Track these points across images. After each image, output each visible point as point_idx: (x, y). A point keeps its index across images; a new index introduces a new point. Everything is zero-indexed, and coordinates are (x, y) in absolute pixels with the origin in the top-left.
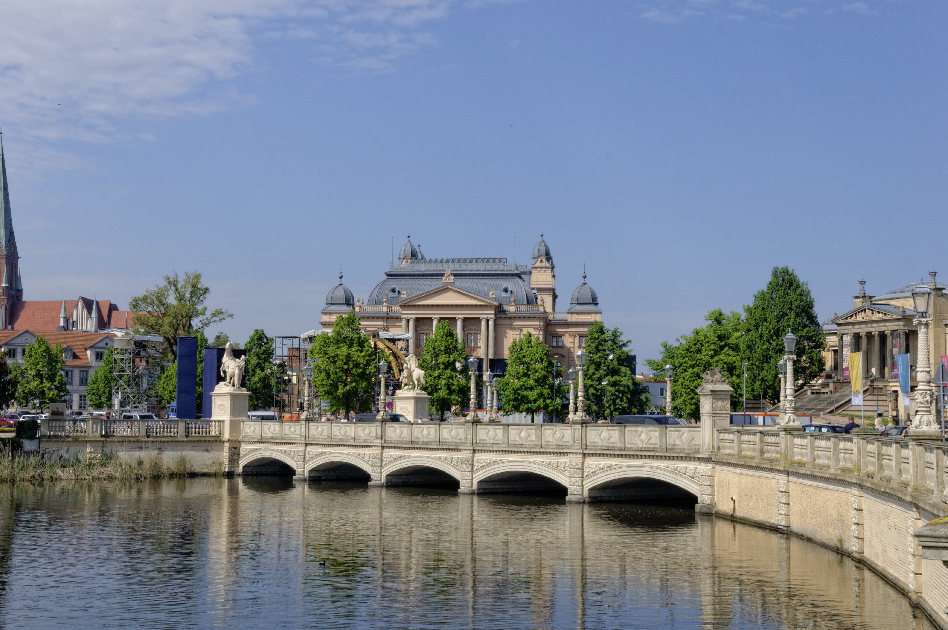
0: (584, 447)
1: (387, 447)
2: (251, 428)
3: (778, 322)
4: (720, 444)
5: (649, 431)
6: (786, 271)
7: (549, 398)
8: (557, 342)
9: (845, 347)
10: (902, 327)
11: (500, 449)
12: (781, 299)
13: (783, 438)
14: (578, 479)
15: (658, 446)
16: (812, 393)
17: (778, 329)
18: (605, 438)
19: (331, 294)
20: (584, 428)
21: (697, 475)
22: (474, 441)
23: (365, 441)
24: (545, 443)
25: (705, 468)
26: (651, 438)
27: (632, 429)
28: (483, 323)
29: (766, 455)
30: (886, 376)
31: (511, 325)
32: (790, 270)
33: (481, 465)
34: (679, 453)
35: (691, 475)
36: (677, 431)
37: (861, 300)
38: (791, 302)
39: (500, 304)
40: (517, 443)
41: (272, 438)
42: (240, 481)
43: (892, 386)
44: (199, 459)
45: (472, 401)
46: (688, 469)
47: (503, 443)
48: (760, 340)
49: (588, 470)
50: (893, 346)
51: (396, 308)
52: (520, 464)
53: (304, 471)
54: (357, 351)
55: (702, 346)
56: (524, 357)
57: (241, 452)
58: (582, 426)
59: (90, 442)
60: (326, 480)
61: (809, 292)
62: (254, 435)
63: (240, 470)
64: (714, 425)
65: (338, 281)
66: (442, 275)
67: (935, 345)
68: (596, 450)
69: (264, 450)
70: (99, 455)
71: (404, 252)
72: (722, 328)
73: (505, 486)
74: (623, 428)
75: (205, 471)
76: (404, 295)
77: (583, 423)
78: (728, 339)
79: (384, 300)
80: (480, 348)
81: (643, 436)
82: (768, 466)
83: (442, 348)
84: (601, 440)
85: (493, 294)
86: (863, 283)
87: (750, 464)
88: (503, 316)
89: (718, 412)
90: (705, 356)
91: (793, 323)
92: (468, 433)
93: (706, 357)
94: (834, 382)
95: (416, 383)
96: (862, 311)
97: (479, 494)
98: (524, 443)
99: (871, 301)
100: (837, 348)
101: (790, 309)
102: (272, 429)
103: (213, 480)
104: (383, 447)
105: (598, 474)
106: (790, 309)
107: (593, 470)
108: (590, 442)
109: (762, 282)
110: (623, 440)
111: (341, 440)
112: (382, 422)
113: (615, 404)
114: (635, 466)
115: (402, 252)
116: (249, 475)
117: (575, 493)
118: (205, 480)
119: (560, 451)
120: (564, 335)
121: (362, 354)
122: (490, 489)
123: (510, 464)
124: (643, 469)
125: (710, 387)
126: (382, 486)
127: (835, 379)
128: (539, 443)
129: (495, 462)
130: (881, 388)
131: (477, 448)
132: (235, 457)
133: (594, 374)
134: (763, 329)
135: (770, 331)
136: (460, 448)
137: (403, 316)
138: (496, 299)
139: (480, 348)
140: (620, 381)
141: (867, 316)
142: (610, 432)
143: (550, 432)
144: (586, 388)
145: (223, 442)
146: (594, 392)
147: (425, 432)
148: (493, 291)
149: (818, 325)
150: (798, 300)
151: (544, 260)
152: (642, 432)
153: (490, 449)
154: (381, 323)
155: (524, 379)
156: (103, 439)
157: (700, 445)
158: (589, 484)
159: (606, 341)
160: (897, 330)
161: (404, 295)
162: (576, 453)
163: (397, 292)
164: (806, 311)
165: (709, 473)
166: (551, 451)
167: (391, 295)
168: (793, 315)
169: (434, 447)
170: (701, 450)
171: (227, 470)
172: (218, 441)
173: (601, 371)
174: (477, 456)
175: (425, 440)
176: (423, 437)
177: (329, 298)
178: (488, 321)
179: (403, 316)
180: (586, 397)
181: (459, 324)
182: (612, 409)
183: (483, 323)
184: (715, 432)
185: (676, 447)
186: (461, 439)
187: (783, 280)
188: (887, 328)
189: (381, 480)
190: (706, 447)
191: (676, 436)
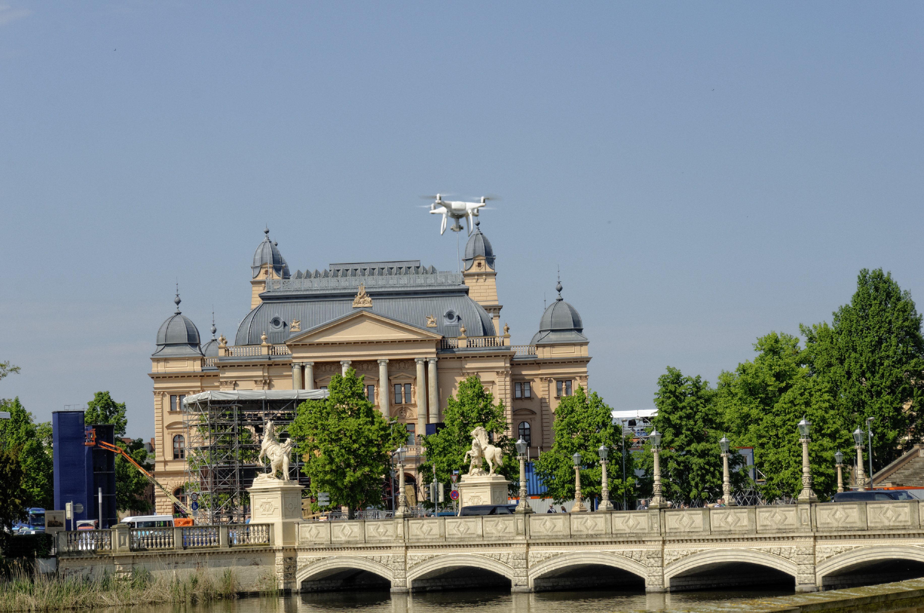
1: (534, 544)
2: (310, 532)
3: (873, 352)
6: (879, 276)
7: (618, 478)
8: (522, 392)
11: (700, 538)
12: (876, 319)
14: (809, 566)
15: (909, 523)
17: (874, 362)
18: (841, 518)
19: (164, 329)
20: (813, 508)
22: (663, 530)
23: (500, 538)
24: (761, 528)
26: (899, 515)
27: (876, 506)
28: (419, 367)
31: (461, 368)
33: (675, 558)
38: (890, 321)
39: (443, 337)
40: (723, 529)
41: (348, 542)
42: (298, 601)
44: (248, 576)
45: (656, 483)
47: (704, 531)
48: (849, 378)
49: (821, 555)
51: (282, 349)
52: (729, 553)
53: (405, 581)
54: (366, 423)
55: (811, 395)
56: (578, 422)
57: (299, 564)
58: (811, 506)
59: (118, 557)
60: (432, 591)
61: (913, 306)
62: (318, 541)
63: (298, 586)
65: (174, 309)
66: (352, 295)
68: (831, 532)
69: (337, 558)
70: (130, 574)
71: (262, 258)
72: (781, 362)
73: (698, 583)
75: (255, 589)
76: (295, 327)
77: (811, 502)
78: (791, 378)
79: (263, 337)
80: (415, 405)
81: (890, 514)
83: (474, 415)
85: (432, 322)
88: (448, 355)
90: (817, 410)
91: (895, 353)
92: (654, 521)
93: (819, 411)
95: (491, 464)
97: (672, 592)
98: (732, 528)
101: (889, 331)
102: (347, 530)
103: (264, 601)
104: (528, 545)
105: (834, 559)
106: (889, 331)
107: (828, 555)
108: (821, 524)
110: (864, 519)
111: (461, 539)
112: (526, 513)
113: (704, 481)
114: (882, 547)
115: (258, 257)
116: (309, 592)
117: (806, 581)
118: (256, 601)
119: (783, 535)
120: (533, 380)
121: (374, 428)
122: (682, 586)
123: (716, 554)
124: (893, 549)
126: (530, 592)
128: (754, 528)
129: (694, 553)
131: (667, 539)
132: (291, 571)
133: (672, 441)
134: (850, 363)
135: (862, 366)
136: (644, 539)
137: (294, 361)
138: (437, 329)
139: (415, 405)
140: (709, 450)
142: (846, 511)
143: (767, 514)
144: (664, 462)
145: (274, 551)
146: (675, 465)
147: (589, 523)
148: (431, 316)
150: (901, 318)
151: (483, 262)
152: (888, 509)
153: (686, 538)
154: (260, 373)
155: (582, 452)
156: (134, 554)
158: (823, 571)
159: (684, 394)
161: (295, 327)
163: (281, 324)
166: (771, 536)
167: (272, 328)
168: (894, 341)
169: (605, 540)
171: (282, 587)
172: (267, 550)
173: (682, 437)
174: (668, 548)
175: (590, 532)
176: (588, 530)
177: (162, 336)
178: (426, 364)
179: (294, 361)
180: (664, 475)
181: (382, 370)
182: (700, 489)
183: (419, 367)
186: (644, 529)
187: (877, 289)
189: (528, 585)
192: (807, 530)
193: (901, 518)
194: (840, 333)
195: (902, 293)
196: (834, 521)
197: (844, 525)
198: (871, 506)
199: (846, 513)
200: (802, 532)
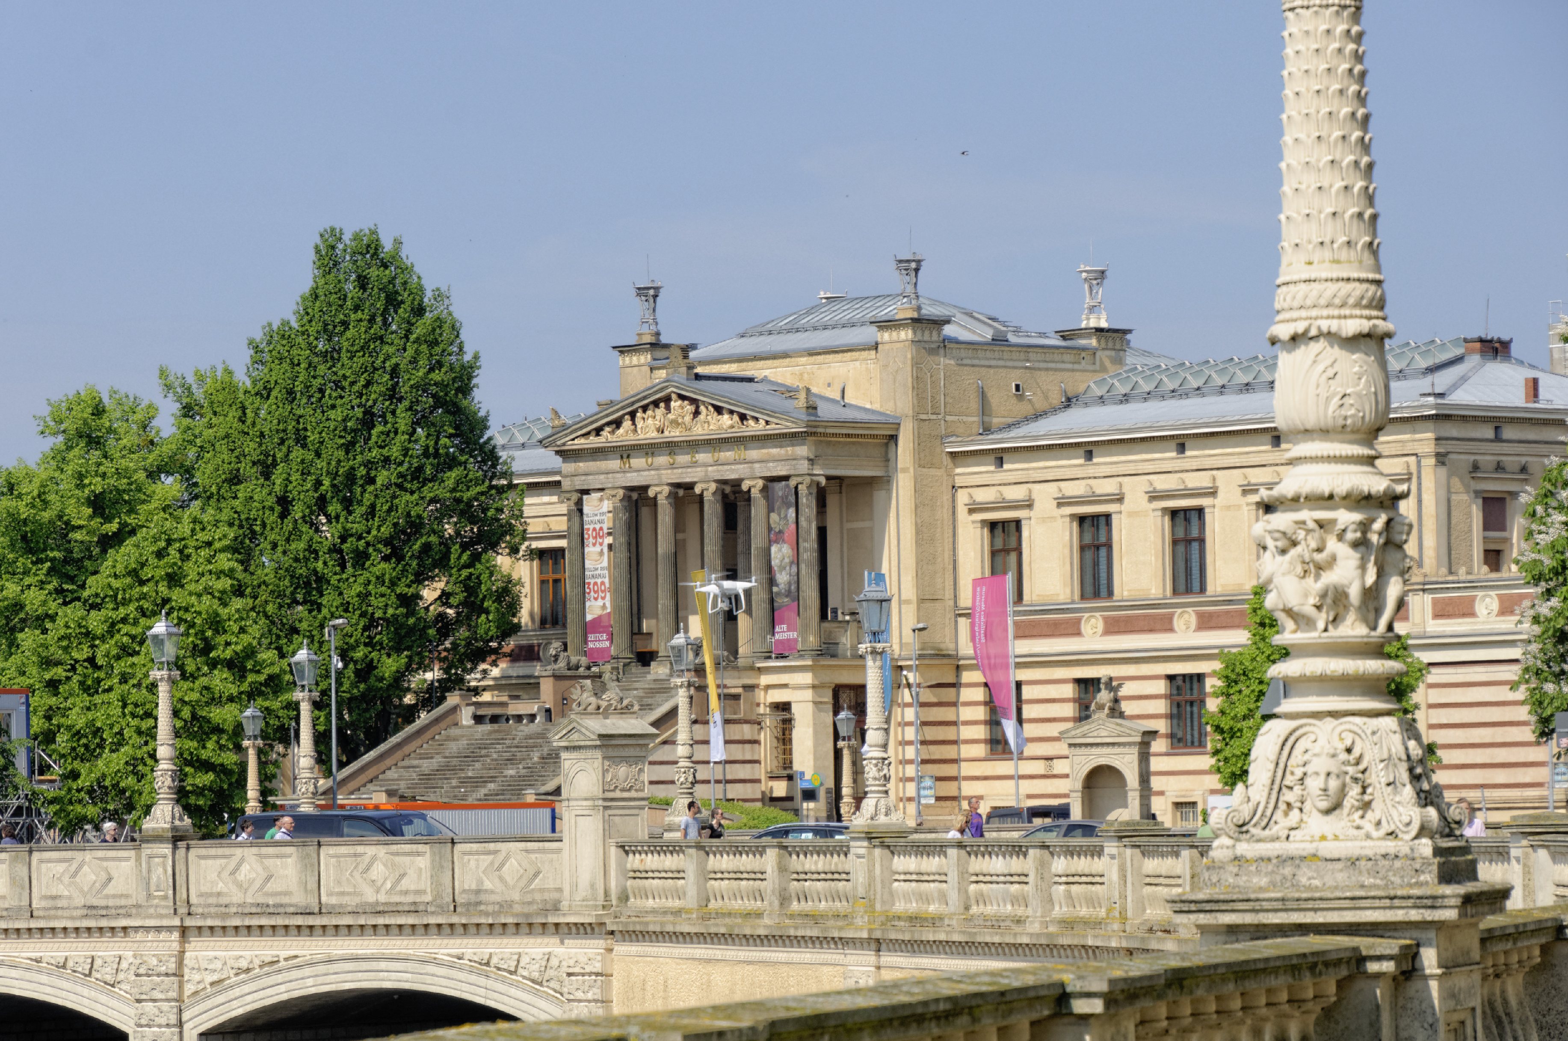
0: (183, 910)
4: (630, 883)
5: (397, 854)
6: (370, 248)
9: (589, 541)
10: (803, 466)
12: (359, 361)
13: (859, 856)
14: (165, 1006)
15: (428, 898)
16: (478, 719)
17: (351, 477)
18: (251, 882)
20: (181, 852)
21: (550, 973)
24: (44, 904)
25: (583, 952)
26: (403, 875)
27: (343, 850)
29: (795, 906)
30: (743, 650)
32: (387, 245)
34: (494, 914)
35: (536, 975)
36: (489, 853)
37: (645, 358)
43: (768, 687)
46: (524, 961)
48: (283, 516)
49: (197, 977)
50: (774, 536)
55: (186, 558)
58: (175, 848)
61: (455, 329)
64: (607, 832)
67: (918, 532)
72: (108, 467)
74: (312, 850)
77: (177, 838)
78: (132, 511)
81: (378, 871)
82: (815, 933)
84: (240, 886)
86: (650, 294)
87: (748, 932)
89: (618, 794)
90: (199, 595)
91: (406, 452)
94: (557, 677)
96: (656, 404)
99: (690, 368)
100: (562, 543)
101: (393, 395)
106: (393, 395)
107: (215, 977)
108: (201, 895)
109: (282, 290)
110: (312, 884)
119: (101, 923)
125: (596, 725)
127: (562, 664)
128: (25, 902)
130: (736, 697)
135: (318, 483)
141: (675, 423)
142: (269, 862)
143: (61, 868)
149: (490, 456)
150: (423, 362)
152: (374, 858)
157: (560, 890)
160: (786, 478)
162: (158, 929)
164: (451, 405)
165: (597, 967)
166: (70, 924)
168: (403, 420)
170: (565, 904)
184: (613, 851)
185: (483, 897)
187: (363, 282)
188: (751, 468)
190: (583, 891)
191: (484, 865)
192: (164, 911)
193: (405, 884)
194: (265, 393)
195: (429, 294)
196: (234, 889)
197: (261, 900)
198: (332, 850)
199: (265, 868)
200: (150, 917)
